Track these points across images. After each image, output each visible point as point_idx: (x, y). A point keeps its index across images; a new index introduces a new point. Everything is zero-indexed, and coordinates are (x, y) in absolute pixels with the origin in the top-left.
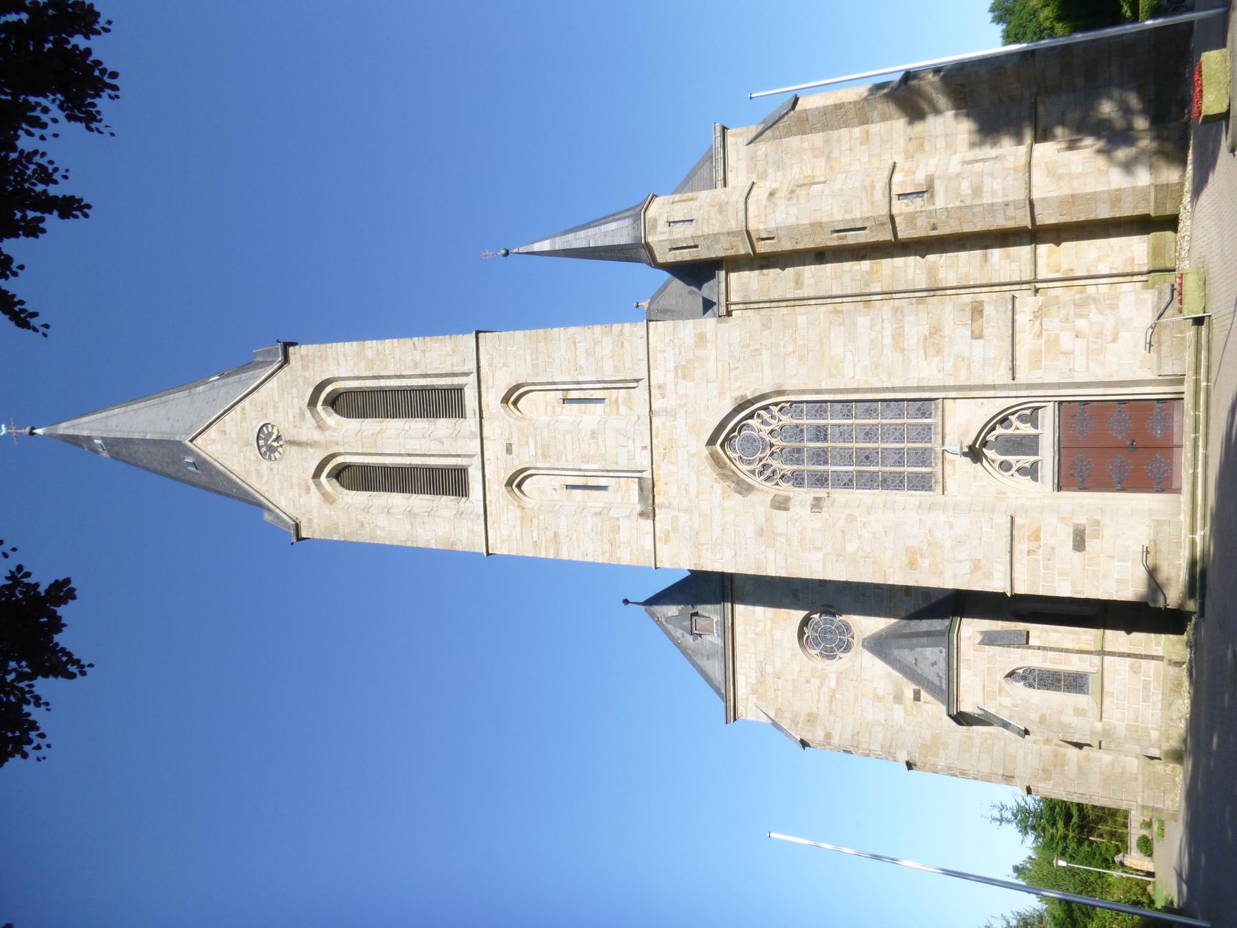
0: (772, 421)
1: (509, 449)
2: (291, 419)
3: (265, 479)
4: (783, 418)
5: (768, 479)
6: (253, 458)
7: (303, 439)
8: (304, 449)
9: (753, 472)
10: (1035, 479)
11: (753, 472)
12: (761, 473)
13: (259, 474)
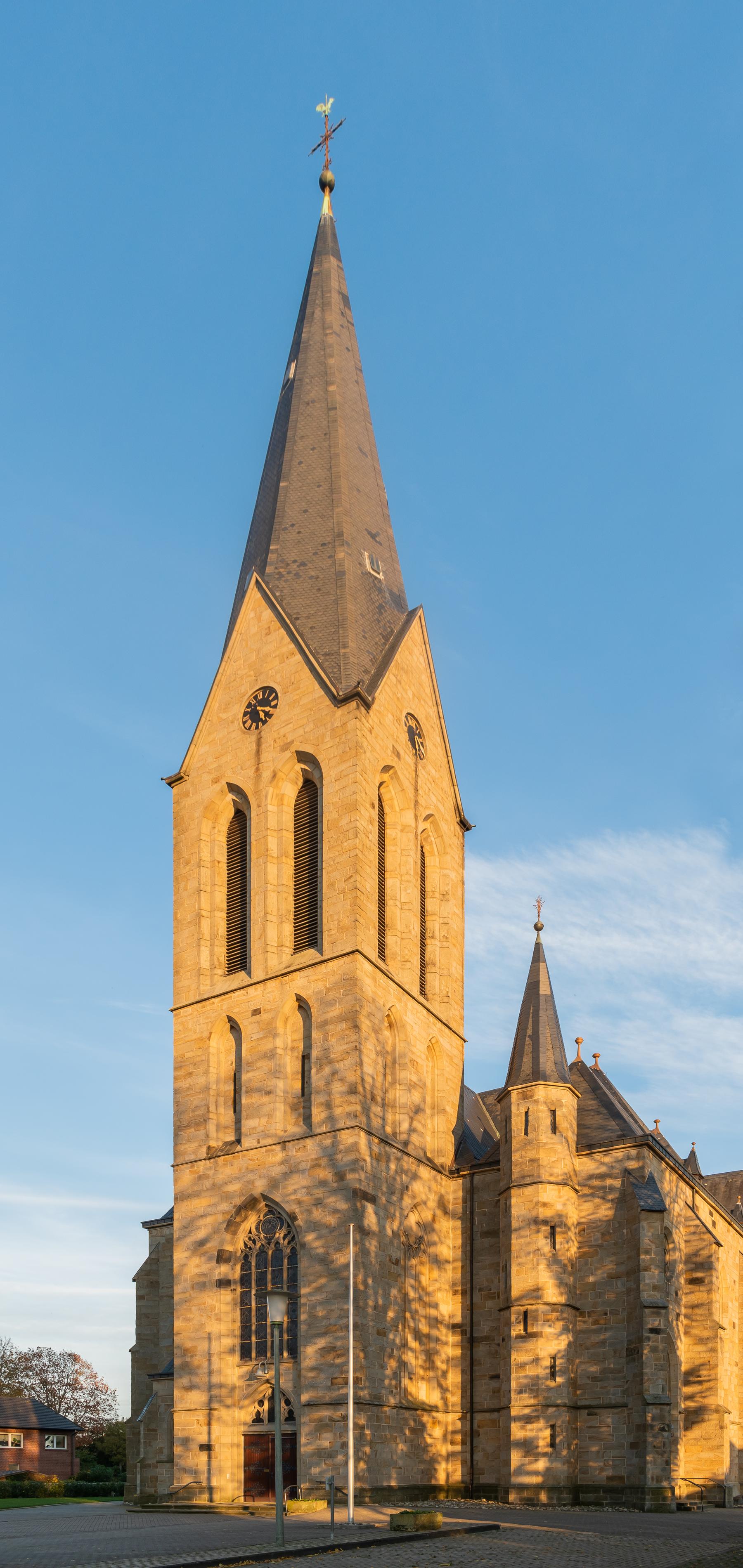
0: (286, 1241)
1: (256, 1012)
2: (282, 731)
3: (224, 716)
4: (289, 1251)
5: (246, 1245)
6: (243, 689)
7: (264, 756)
8: (253, 761)
9: (250, 1232)
10: (254, 1421)
11: (250, 1232)
12: (250, 1239)
13: (226, 707)
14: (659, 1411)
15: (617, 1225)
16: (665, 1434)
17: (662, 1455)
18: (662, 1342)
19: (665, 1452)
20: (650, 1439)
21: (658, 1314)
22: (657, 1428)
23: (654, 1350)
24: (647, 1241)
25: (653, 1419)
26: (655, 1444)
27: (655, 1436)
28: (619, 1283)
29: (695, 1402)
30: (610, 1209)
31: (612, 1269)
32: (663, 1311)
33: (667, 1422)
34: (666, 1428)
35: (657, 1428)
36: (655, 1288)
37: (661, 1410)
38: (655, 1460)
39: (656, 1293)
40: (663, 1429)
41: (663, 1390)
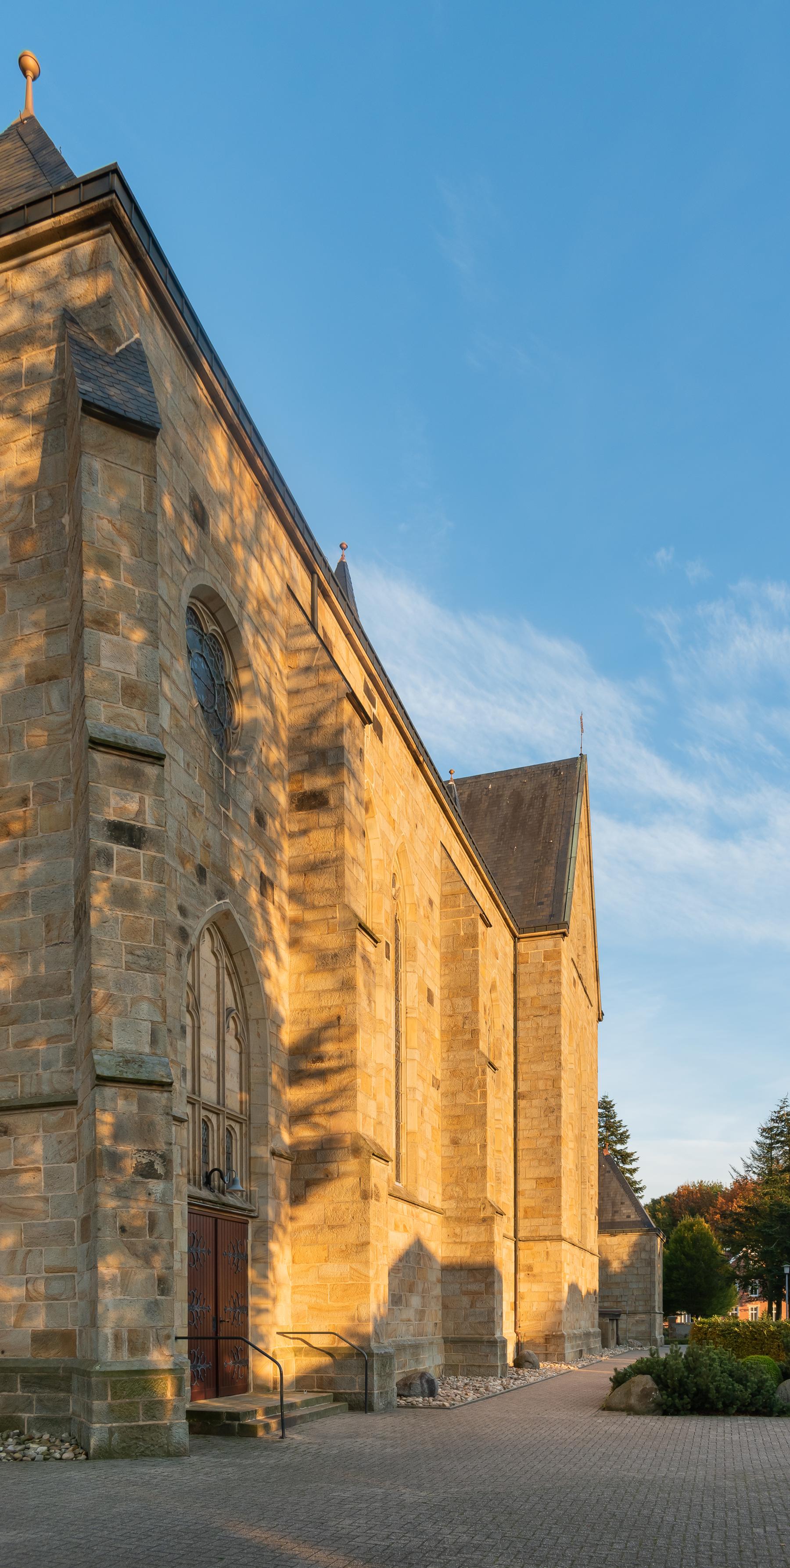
14: (134, 1108)
15: (47, 502)
16: (157, 1186)
17: (147, 1261)
18: (150, 875)
19: (155, 1249)
20: (110, 1204)
21: (136, 780)
22: (129, 1165)
23: (124, 898)
24: (105, 525)
25: (118, 1135)
26: (125, 1217)
27: (121, 1194)
28: (55, 696)
29: (316, 1126)
30: (30, 447)
31: (38, 650)
32: (151, 771)
33: (161, 1147)
34: (159, 1168)
35: (129, 1165)
36: (131, 692)
37: (143, 1104)
38: (125, 1275)
39: (135, 713)
40: (147, 1172)
41: (154, 1042)
